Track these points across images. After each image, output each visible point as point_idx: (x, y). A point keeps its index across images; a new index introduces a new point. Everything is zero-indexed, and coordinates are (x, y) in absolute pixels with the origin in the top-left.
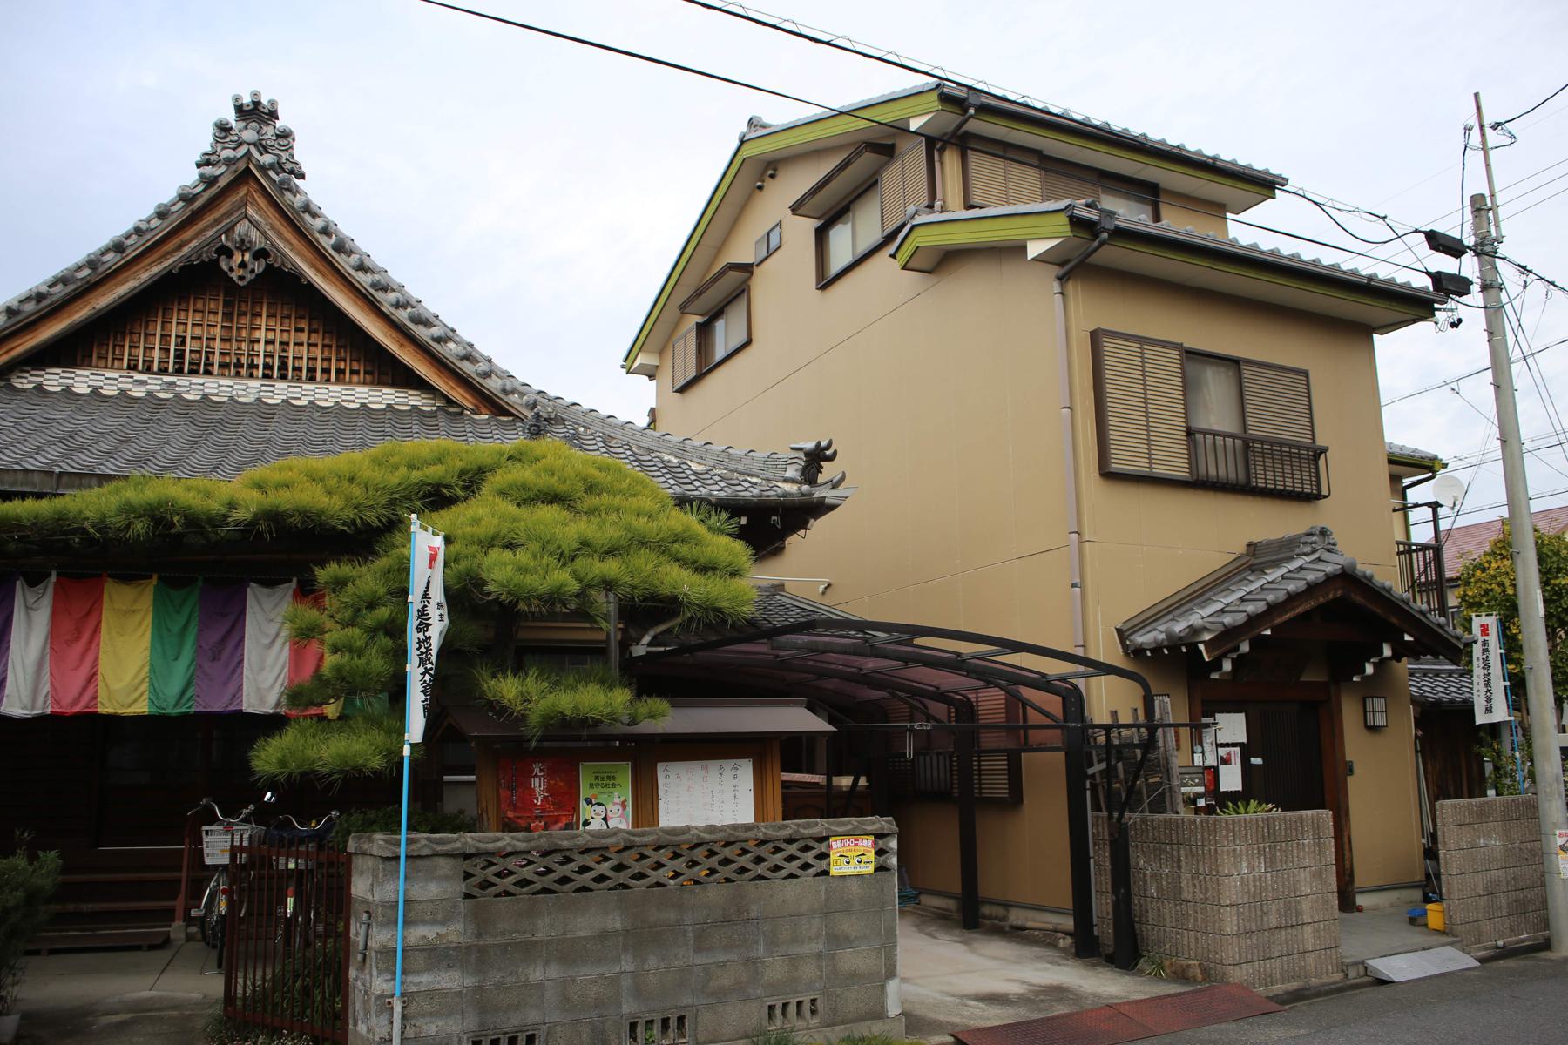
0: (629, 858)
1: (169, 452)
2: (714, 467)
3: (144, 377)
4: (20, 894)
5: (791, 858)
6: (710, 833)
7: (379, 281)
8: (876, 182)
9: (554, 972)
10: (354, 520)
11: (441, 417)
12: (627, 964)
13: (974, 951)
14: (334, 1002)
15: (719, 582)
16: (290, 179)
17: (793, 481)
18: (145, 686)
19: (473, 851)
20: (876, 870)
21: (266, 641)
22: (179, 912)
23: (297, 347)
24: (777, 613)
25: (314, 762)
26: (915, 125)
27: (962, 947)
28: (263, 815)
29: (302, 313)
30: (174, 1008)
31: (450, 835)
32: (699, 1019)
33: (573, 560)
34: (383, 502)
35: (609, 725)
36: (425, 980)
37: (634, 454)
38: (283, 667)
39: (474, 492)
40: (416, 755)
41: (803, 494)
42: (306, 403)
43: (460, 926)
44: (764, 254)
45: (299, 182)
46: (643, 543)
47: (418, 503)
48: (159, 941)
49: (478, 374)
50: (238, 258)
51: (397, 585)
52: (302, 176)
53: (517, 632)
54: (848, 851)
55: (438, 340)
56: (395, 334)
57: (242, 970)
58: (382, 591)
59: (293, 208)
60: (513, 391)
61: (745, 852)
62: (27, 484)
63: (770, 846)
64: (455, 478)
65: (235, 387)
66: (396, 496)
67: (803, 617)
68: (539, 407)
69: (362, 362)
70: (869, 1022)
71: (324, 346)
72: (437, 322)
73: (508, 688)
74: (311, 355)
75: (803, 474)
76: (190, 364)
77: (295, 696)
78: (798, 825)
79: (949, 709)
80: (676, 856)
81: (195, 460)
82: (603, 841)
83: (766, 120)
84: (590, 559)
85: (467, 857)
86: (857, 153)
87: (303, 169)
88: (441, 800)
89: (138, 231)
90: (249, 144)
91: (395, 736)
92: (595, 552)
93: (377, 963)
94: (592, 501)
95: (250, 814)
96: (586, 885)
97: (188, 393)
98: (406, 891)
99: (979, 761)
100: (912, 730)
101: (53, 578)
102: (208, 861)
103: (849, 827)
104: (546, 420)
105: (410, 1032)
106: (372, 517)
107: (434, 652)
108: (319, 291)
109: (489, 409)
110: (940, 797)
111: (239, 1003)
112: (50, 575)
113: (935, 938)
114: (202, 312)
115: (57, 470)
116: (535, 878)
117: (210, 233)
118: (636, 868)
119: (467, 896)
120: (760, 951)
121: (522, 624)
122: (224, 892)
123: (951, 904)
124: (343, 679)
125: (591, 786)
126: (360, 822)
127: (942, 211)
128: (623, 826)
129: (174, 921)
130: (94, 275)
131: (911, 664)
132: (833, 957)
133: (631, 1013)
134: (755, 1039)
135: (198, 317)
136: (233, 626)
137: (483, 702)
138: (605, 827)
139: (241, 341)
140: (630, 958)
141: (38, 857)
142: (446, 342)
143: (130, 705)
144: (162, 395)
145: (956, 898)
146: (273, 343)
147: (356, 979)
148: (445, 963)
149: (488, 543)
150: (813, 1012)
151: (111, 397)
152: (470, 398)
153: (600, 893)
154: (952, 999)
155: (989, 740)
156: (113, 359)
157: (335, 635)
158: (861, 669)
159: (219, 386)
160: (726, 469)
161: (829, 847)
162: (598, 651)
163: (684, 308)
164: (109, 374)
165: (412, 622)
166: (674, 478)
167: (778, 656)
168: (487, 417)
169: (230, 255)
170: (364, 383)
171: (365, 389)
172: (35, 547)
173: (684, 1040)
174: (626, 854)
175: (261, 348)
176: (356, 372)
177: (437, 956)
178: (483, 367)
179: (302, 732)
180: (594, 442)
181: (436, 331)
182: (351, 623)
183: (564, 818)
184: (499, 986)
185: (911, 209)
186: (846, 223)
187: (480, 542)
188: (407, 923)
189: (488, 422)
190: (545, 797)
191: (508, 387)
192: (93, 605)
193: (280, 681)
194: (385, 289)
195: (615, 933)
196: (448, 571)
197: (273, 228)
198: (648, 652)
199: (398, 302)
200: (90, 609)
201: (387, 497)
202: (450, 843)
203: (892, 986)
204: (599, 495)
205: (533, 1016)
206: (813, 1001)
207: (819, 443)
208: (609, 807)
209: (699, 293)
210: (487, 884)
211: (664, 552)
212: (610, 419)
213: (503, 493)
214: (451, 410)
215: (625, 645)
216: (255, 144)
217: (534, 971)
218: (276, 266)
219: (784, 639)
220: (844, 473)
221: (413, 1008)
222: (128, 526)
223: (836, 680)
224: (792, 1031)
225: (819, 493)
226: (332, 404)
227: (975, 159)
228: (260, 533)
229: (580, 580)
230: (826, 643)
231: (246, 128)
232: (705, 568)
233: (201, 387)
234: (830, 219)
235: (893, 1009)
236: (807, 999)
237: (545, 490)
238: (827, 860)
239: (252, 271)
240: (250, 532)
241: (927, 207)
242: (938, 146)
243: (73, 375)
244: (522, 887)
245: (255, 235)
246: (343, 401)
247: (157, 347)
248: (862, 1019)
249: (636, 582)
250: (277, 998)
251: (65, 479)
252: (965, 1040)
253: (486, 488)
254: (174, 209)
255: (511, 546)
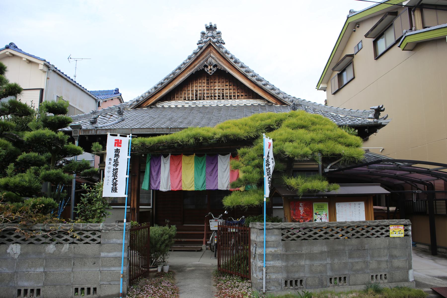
0: (328, 230)
1: (196, 121)
2: (347, 115)
3: (188, 102)
4: (168, 236)
5: (377, 231)
6: (353, 224)
7: (247, 70)
8: (392, 24)
9: (308, 262)
10: (247, 136)
11: (267, 106)
12: (329, 261)
13: (436, 263)
14: (247, 268)
15: (353, 149)
16: (221, 45)
17: (371, 118)
18: (193, 183)
19: (284, 228)
20: (404, 236)
21: (224, 170)
22: (204, 242)
23: (226, 90)
24: (367, 158)
25: (240, 203)
26: (404, 4)
27: (432, 261)
28: (224, 217)
29: (227, 81)
30: (205, 267)
31: (278, 223)
32: (350, 278)
33: (310, 144)
34: (255, 131)
35: (322, 192)
36: (271, 263)
37: (323, 113)
38: (228, 177)
39: (279, 126)
40: (267, 201)
41: (375, 122)
42: (230, 105)
43: (281, 249)
44: (357, 51)
45: (224, 45)
46: (330, 139)
47: (264, 130)
48: (199, 249)
49: (276, 94)
50: (209, 68)
51: (260, 153)
52: (224, 44)
53: (293, 165)
54: (395, 230)
55: (264, 85)
56: (252, 84)
57: (230, 256)
58: (256, 155)
59: (223, 53)
60: (286, 98)
61: (363, 229)
62: (163, 131)
63: (371, 228)
64: (274, 123)
65: (211, 102)
66: (258, 129)
67: (375, 159)
68: (294, 102)
69: (244, 92)
70: (404, 282)
71: (233, 89)
72: (263, 80)
73: (292, 182)
74: (230, 92)
75: (374, 116)
76: (199, 97)
77: (233, 185)
78: (379, 222)
79: (424, 186)
80: (342, 230)
81: (203, 122)
82: (321, 225)
83: (355, 10)
84: (314, 144)
85: (282, 229)
86: (385, 16)
87: (224, 42)
88: (272, 213)
89: (184, 63)
90: (210, 37)
91: (261, 196)
92: (316, 142)
93: (259, 258)
94: (313, 127)
95: (221, 217)
96: (316, 238)
97: (199, 105)
98: (266, 238)
99: (435, 203)
100: (415, 193)
101: (170, 155)
102: (211, 229)
103: (395, 222)
104: (296, 105)
105: (268, 277)
106: (252, 135)
107: (271, 172)
108: (231, 74)
109: (280, 103)
110: (422, 213)
111: (222, 267)
112: (169, 154)
113: (422, 257)
114: (201, 83)
115: (170, 127)
116: (302, 236)
117: (202, 62)
118: (331, 233)
119: (283, 240)
120: (369, 259)
121: (295, 164)
122: (216, 237)
123: (427, 247)
124: (247, 180)
125: (317, 209)
126: (252, 219)
127: (415, 30)
128: (326, 221)
129: (203, 244)
130: (175, 76)
131: (412, 173)
132: (391, 262)
133: (330, 275)
134: (367, 285)
135: (200, 84)
136: (215, 167)
137: (285, 186)
138: (321, 221)
139: (212, 90)
140: (329, 259)
141: (171, 227)
142: (266, 85)
143: (190, 188)
144: (193, 106)
145: (428, 245)
146: (220, 90)
147: (253, 262)
148: (277, 259)
149: (285, 141)
150: (385, 278)
151: (180, 108)
152: (274, 100)
153: (320, 240)
154: (430, 277)
155: (438, 196)
156: (180, 98)
157: (244, 168)
158: (395, 174)
159: (207, 102)
160: (350, 116)
161: (389, 228)
162: (316, 171)
163: (333, 69)
164: (179, 102)
165: (265, 164)
166: (335, 119)
167: (369, 171)
168: (279, 105)
169: (207, 67)
170: (245, 99)
171: (245, 100)
172: (166, 147)
173: (346, 284)
174: (328, 229)
175: (217, 91)
176: (243, 96)
177: (275, 256)
178: (277, 91)
179: (236, 195)
180: (310, 110)
181: (263, 82)
182: (247, 165)
183: (309, 219)
184: (292, 266)
185: (404, 31)
186: (382, 38)
187: (282, 141)
188: (266, 247)
189: (280, 107)
190: (303, 212)
191: (285, 97)
192: (180, 162)
193: (227, 182)
194: (249, 72)
195: (325, 252)
196: (274, 149)
197: (218, 59)
198: (329, 171)
199: (253, 75)
200: (179, 163)
201: (256, 129)
202: (278, 225)
203: (411, 272)
204: (316, 125)
205: (302, 275)
206: (385, 275)
207: (379, 106)
208: (322, 215)
209: (338, 65)
210: (288, 237)
211: (336, 141)
212: (315, 104)
213: (288, 126)
214: (269, 104)
215: (323, 168)
216: (211, 37)
217: (302, 262)
218: (219, 69)
219: (371, 166)
220: (387, 115)
221: (268, 271)
222: (189, 141)
223: (387, 178)
224: (379, 283)
225: (380, 121)
226: (236, 105)
227: (426, 12)
228: (222, 141)
229: (312, 150)
230: (385, 167)
231: (209, 32)
232: (349, 145)
233: (202, 103)
234: (378, 37)
235: (411, 279)
236: (383, 274)
237: (300, 125)
238: (389, 232)
239: (213, 71)
240: (220, 141)
241: (410, 30)
242: (413, 10)
243: (171, 103)
244: (331, 237)
245: (213, 61)
246: (239, 104)
247: (190, 93)
248: (401, 281)
249: (328, 150)
250: (232, 266)
251: (171, 130)
252: (436, 291)
253: (283, 125)
254: (192, 56)
255: (291, 141)
